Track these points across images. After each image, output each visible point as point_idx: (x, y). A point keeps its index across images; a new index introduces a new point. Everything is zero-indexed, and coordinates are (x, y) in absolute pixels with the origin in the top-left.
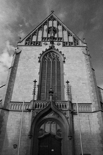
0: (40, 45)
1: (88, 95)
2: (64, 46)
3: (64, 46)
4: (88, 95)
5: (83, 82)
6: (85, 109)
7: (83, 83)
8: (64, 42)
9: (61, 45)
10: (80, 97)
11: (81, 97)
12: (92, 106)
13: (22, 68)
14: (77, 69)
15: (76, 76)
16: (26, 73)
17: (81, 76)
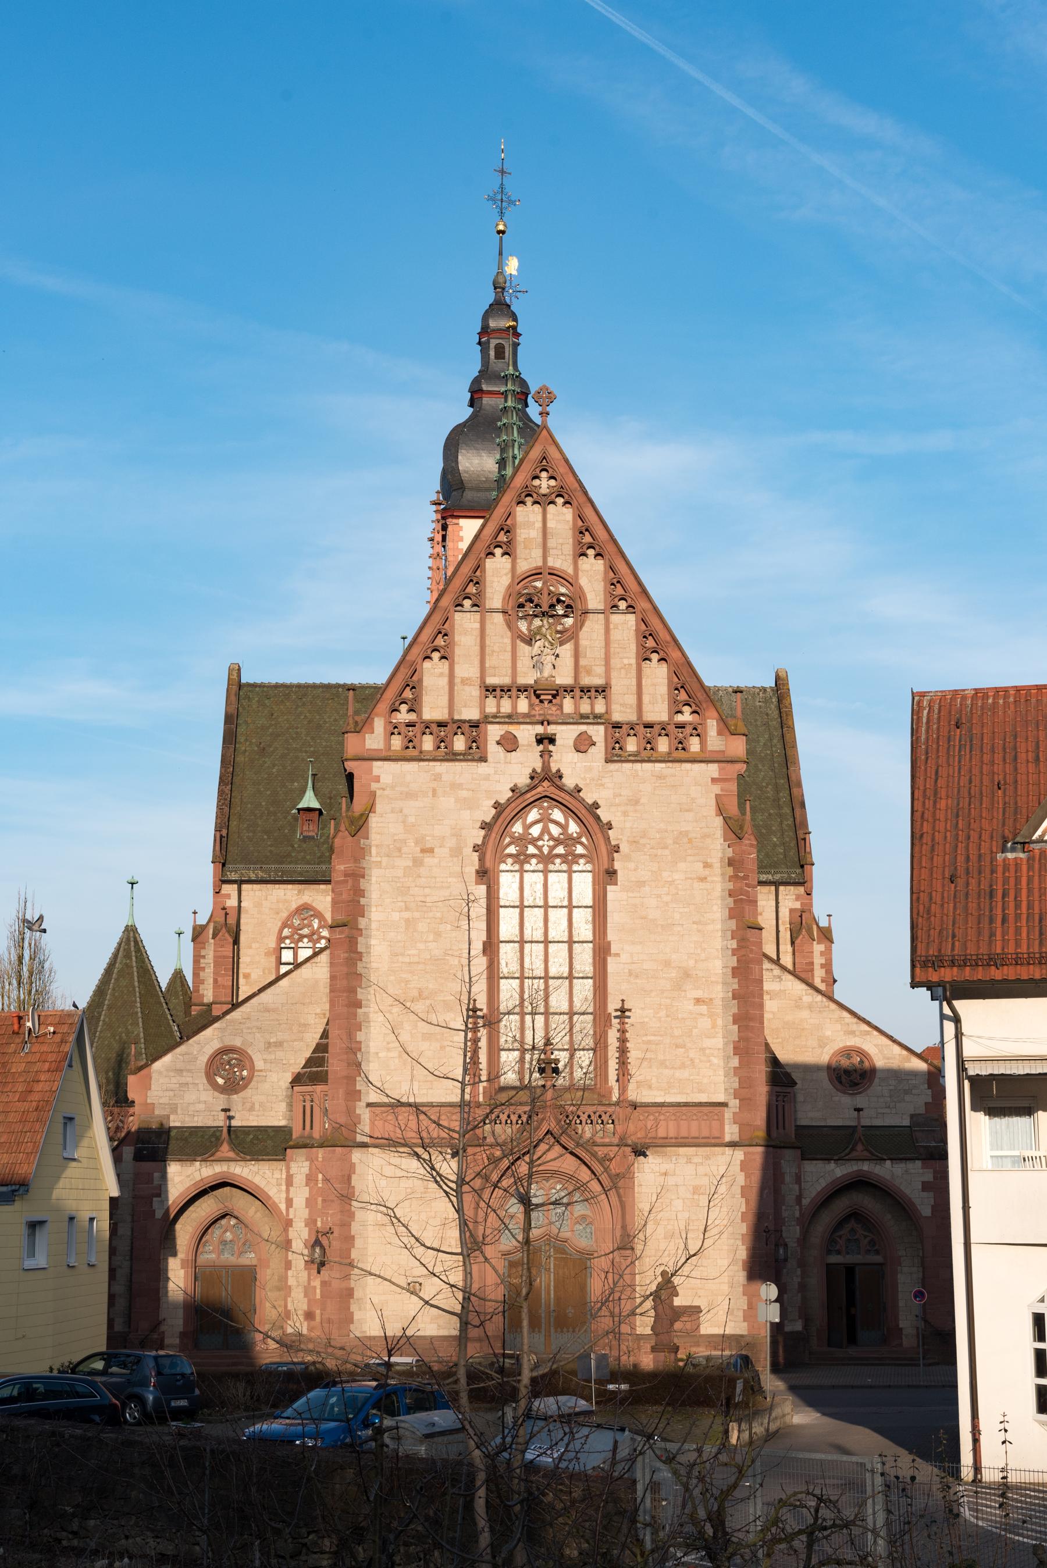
0: (476, 753)
1: (715, 1061)
2: (615, 754)
3: (615, 754)
4: (715, 1061)
5: (699, 994)
6: (694, 1128)
7: (698, 1001)
8: (617, 726)
9: (598, 752)
10: (679, 1074)
11: (684, 1074)
12: (728, 1114)
13: (396, 916)
14: (677, 916)
15: (667, 963)
16: (421, 946)
17: (691, 963)
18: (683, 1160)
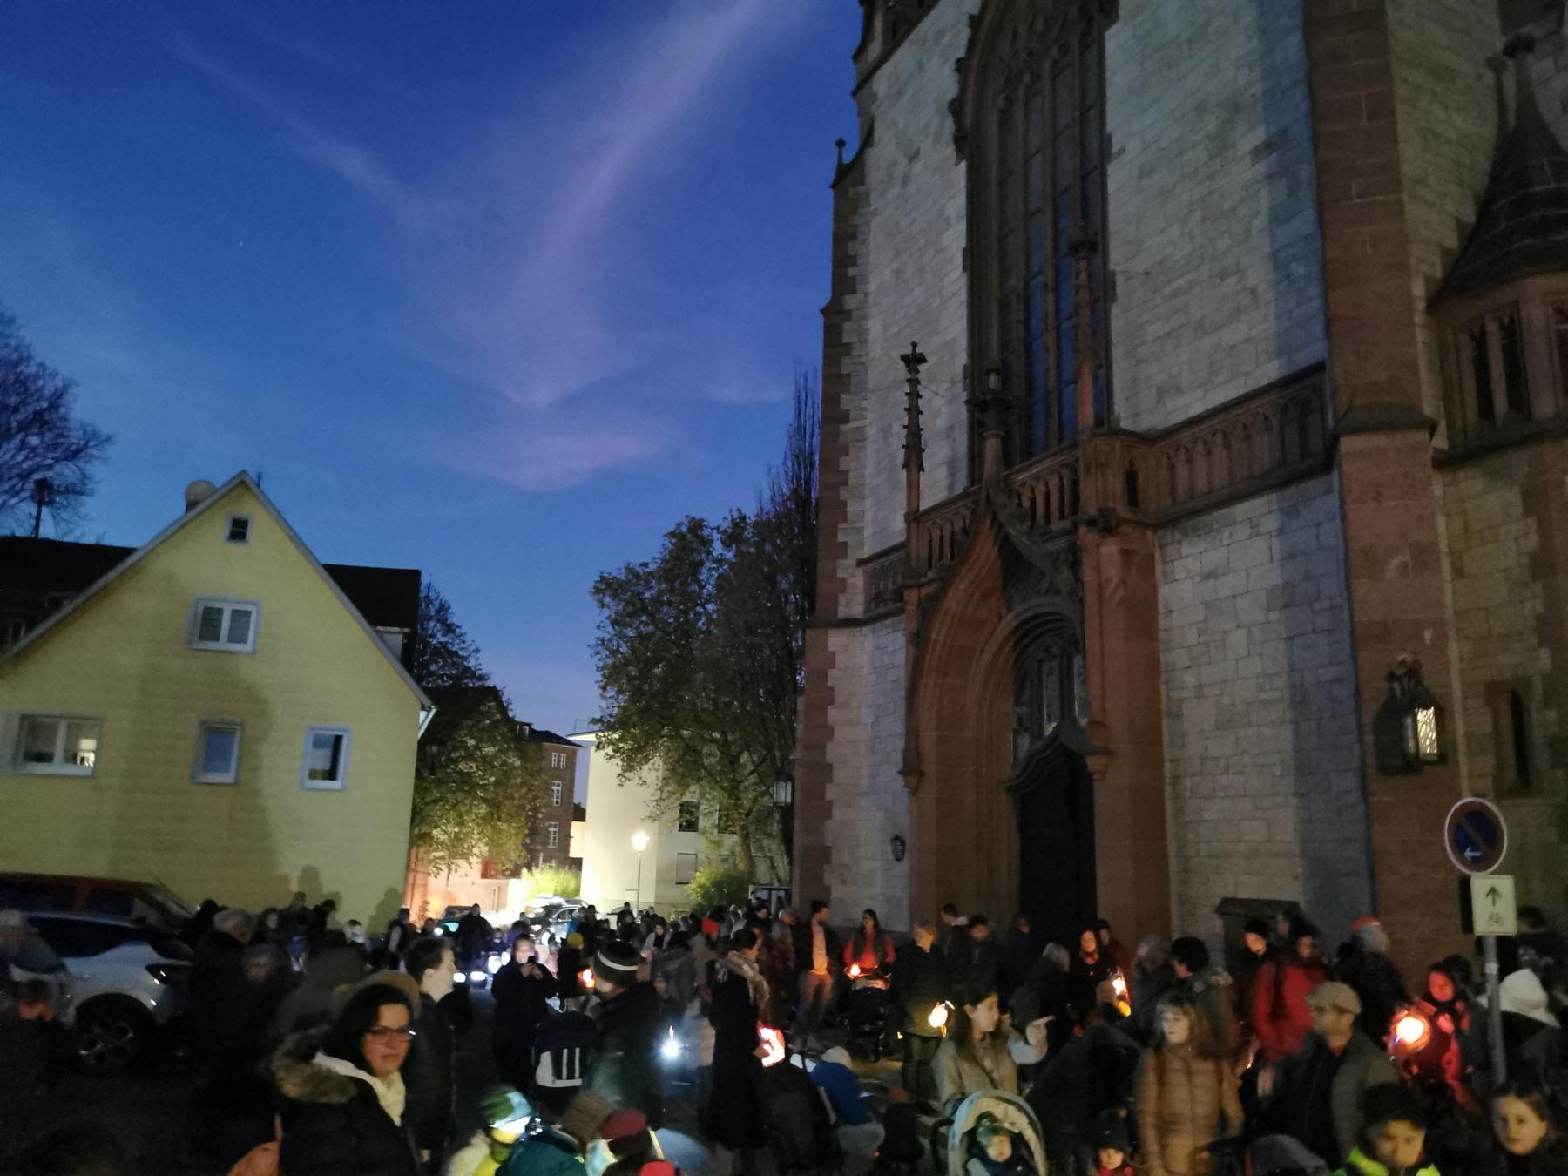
18: (1243, 532)
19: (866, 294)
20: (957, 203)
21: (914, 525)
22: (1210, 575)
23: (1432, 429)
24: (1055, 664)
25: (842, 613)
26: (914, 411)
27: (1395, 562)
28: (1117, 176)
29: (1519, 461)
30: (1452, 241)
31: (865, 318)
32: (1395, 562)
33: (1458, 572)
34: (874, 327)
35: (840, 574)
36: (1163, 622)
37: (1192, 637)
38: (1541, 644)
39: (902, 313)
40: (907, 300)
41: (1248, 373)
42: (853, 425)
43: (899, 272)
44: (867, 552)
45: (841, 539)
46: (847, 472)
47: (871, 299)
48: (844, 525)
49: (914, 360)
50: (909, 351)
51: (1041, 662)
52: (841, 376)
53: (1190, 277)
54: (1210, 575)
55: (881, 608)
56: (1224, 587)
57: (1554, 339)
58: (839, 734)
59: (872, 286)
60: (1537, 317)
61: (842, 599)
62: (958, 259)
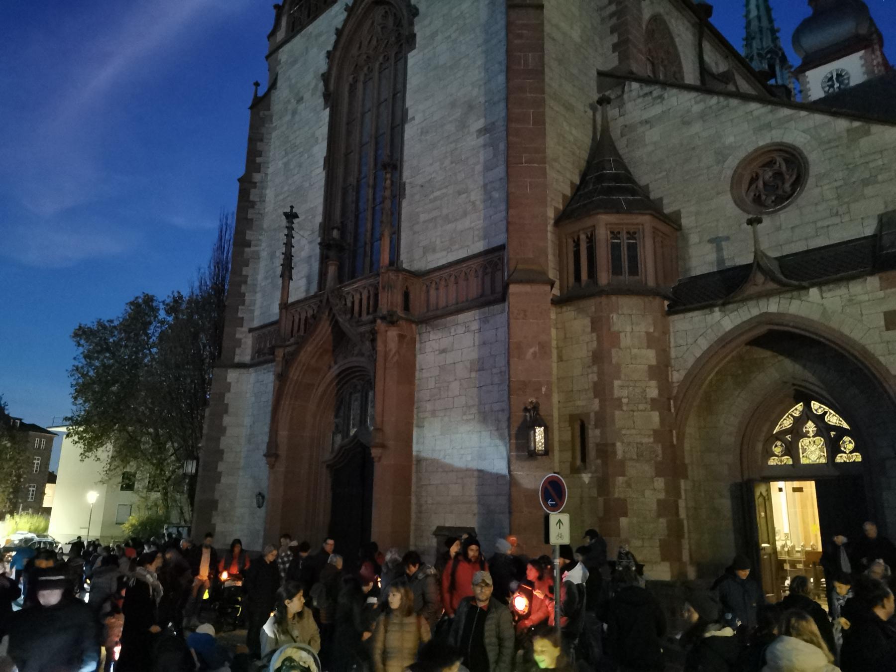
19: (266, 174)
20: (323, 131)
21: (284, 311)
22: (444, 351)
23: (552, 285)
24: (358, 395)
25: (237, 359)
26: (289, 245)
27: (532, 350)
28: (410, 131)
29: (591, 305)
30: (568, 192)
31: (264, 188)
32: (532, 350)
33: (560, 359)
34: (270, 193)
35: (238, 336)
36: (417, 374)
37: (432, 384)
38: (595, 397)
39: (286, 188)
40: (290, 181)
41: (468, 246)
42: (253, 249)
43: (286, 165)
44: (256, 324)
45: (240, 315)
46: (247, 276)
47: (269, 178)
48: (243, 307)
49: (291, 216)
50: (288, 210)
51: (351, 394)
52: (246, 219)
53: (444, 191)
54: (444, 351)
55: (261, 358)
56: (450, 358)
57: (610, 246)
58: (228, 432)
59: (270, 171)
60: (602, 234)
61: (238, 351)
62: (322, 162)
